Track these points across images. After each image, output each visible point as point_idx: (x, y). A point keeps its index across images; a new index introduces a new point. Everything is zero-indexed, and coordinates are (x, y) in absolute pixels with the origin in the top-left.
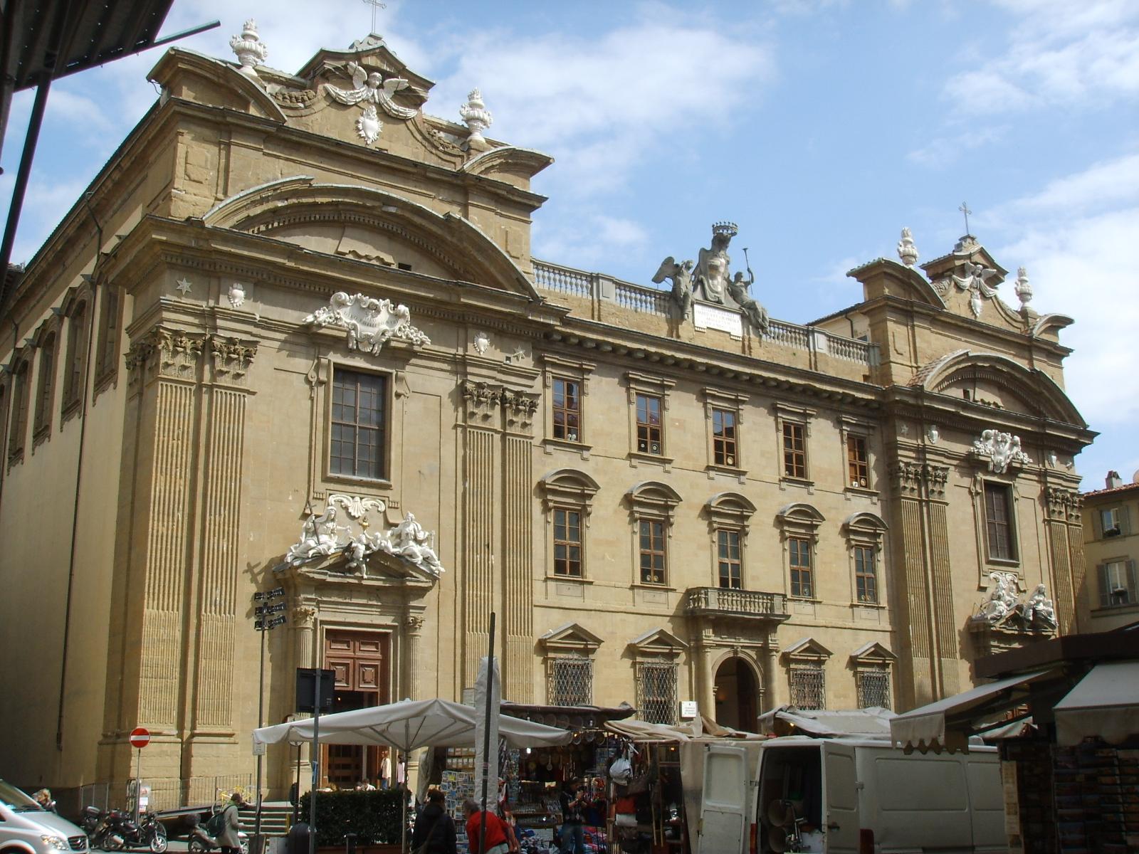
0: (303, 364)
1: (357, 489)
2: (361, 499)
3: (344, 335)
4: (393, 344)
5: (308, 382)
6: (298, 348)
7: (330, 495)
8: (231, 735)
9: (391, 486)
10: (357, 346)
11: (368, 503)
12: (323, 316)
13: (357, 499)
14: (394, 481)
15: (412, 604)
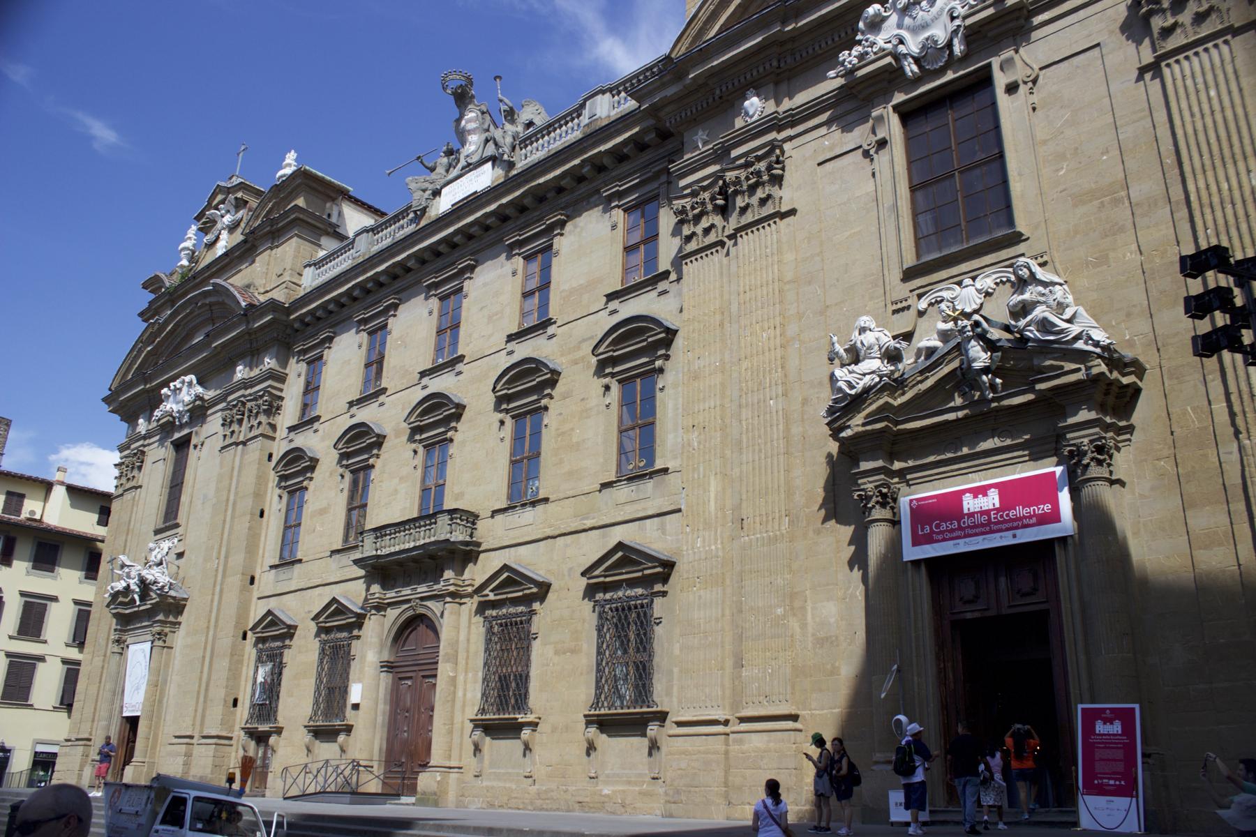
0: (860, 135)
1: (964, 267)
2: (974, 279)
3: (889, 60)
4: (969, 21)
5: (866, 154)
6: (851, 118)
7: (920, 296)
8: (794, 718)
9: (1021, 234)
10: (920, 67)
11: (986, 282)
12: (849, 57)
13: (968, 281)
14: (1021, 225)
15: (1071, 421)
